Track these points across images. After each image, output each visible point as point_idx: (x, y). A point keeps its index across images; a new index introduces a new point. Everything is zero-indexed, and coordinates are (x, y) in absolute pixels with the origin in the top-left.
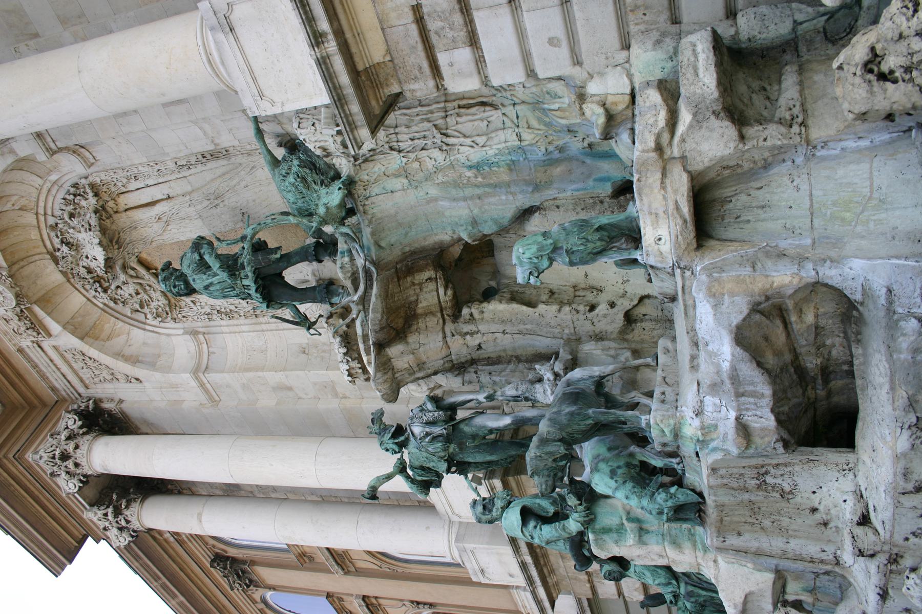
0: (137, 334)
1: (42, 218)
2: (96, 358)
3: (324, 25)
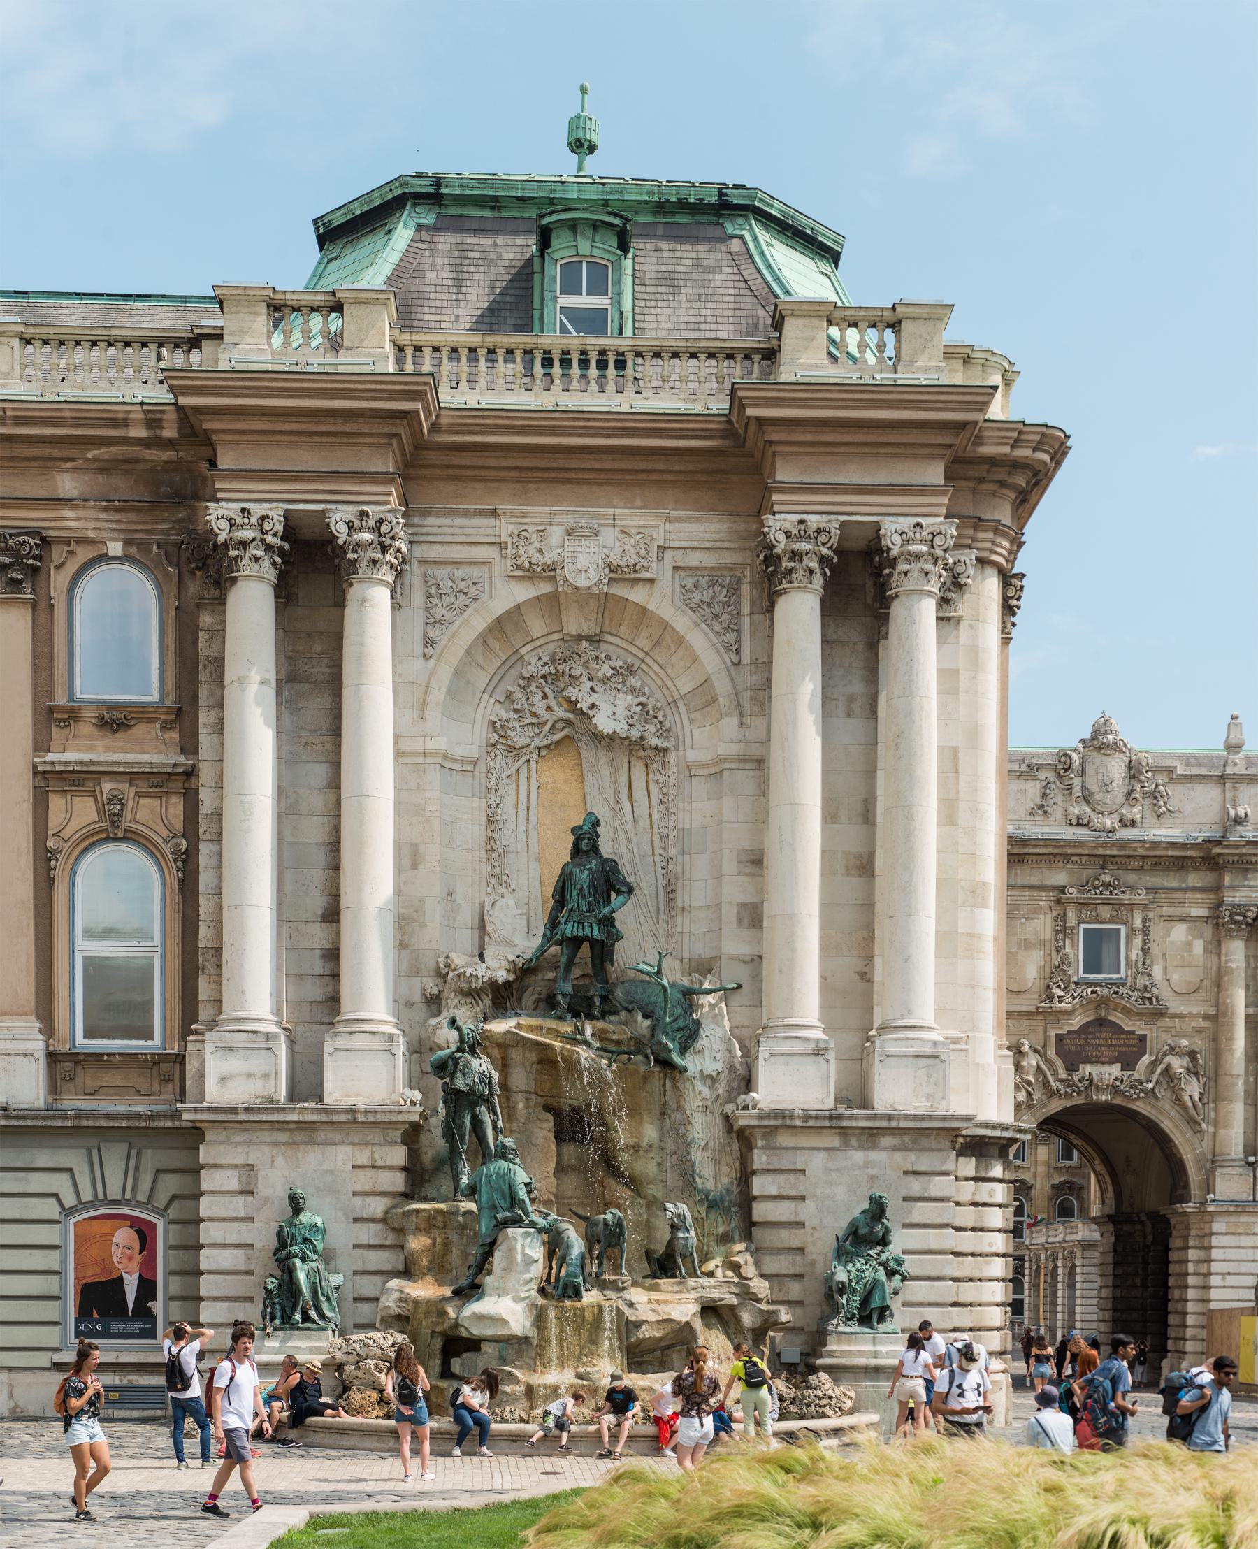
0: (481, 679)
1: (641, 655)
2: (466, 615)
3: (811, 1123)
